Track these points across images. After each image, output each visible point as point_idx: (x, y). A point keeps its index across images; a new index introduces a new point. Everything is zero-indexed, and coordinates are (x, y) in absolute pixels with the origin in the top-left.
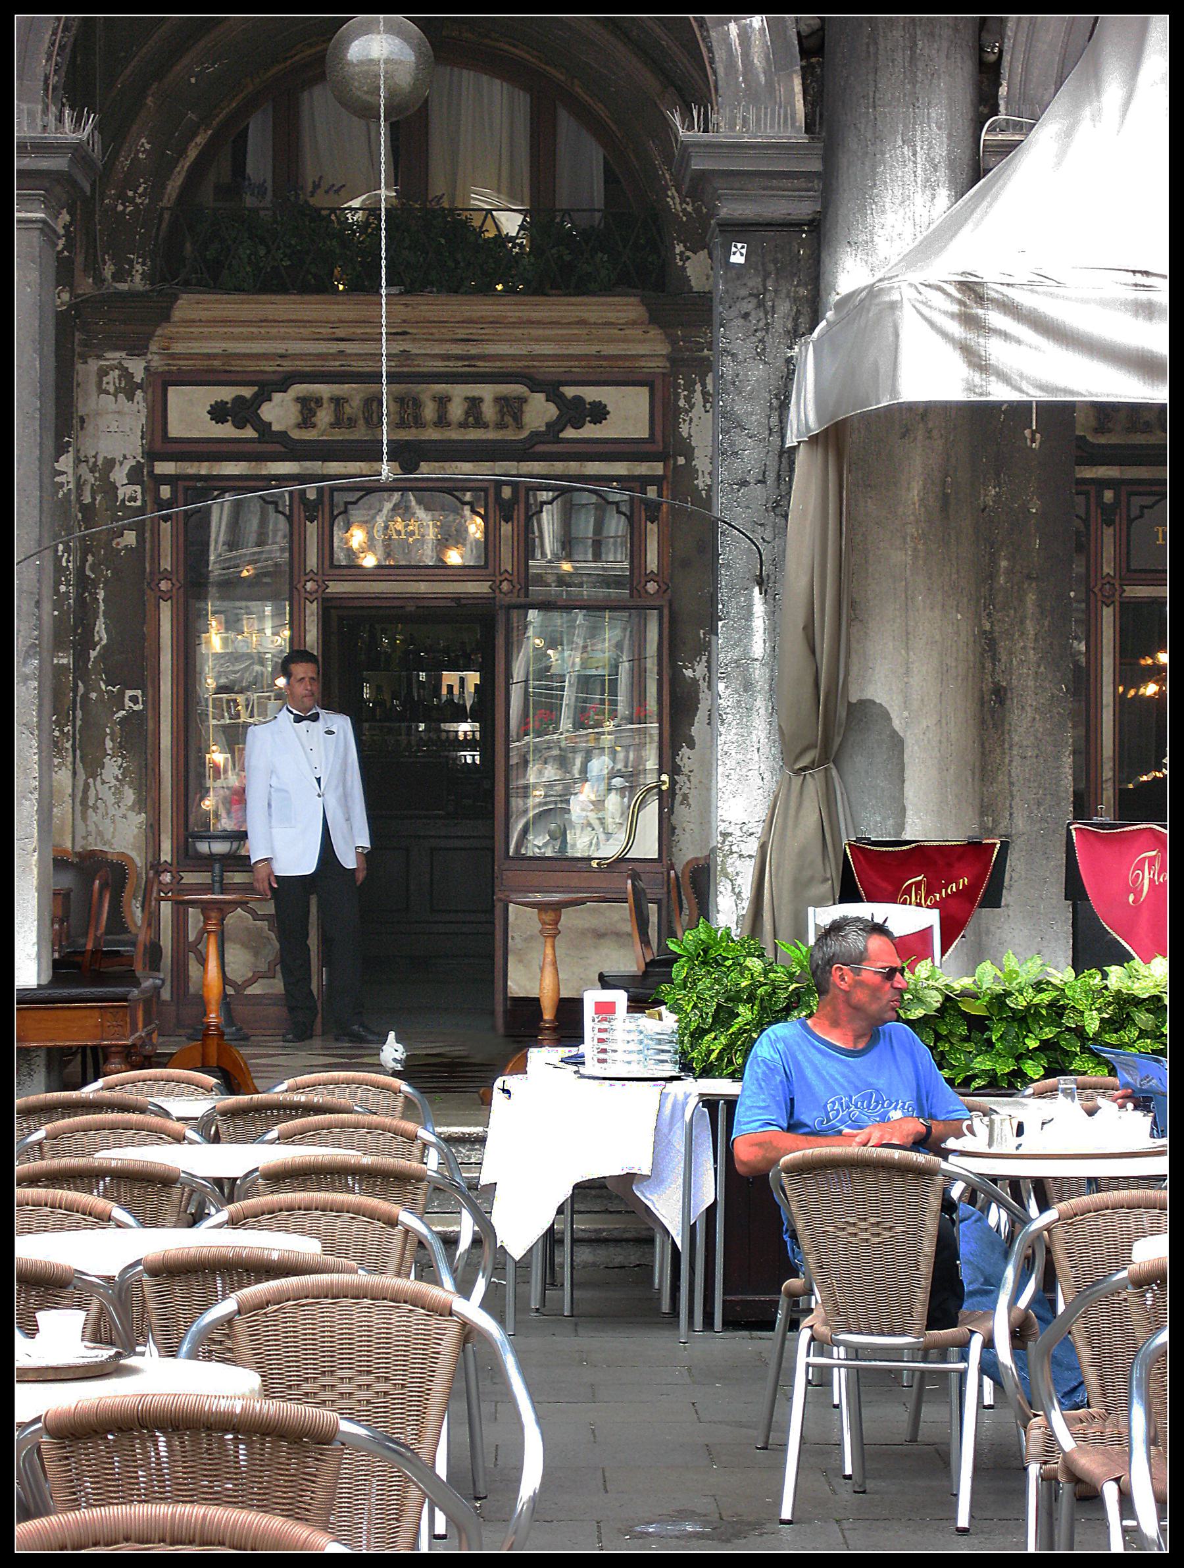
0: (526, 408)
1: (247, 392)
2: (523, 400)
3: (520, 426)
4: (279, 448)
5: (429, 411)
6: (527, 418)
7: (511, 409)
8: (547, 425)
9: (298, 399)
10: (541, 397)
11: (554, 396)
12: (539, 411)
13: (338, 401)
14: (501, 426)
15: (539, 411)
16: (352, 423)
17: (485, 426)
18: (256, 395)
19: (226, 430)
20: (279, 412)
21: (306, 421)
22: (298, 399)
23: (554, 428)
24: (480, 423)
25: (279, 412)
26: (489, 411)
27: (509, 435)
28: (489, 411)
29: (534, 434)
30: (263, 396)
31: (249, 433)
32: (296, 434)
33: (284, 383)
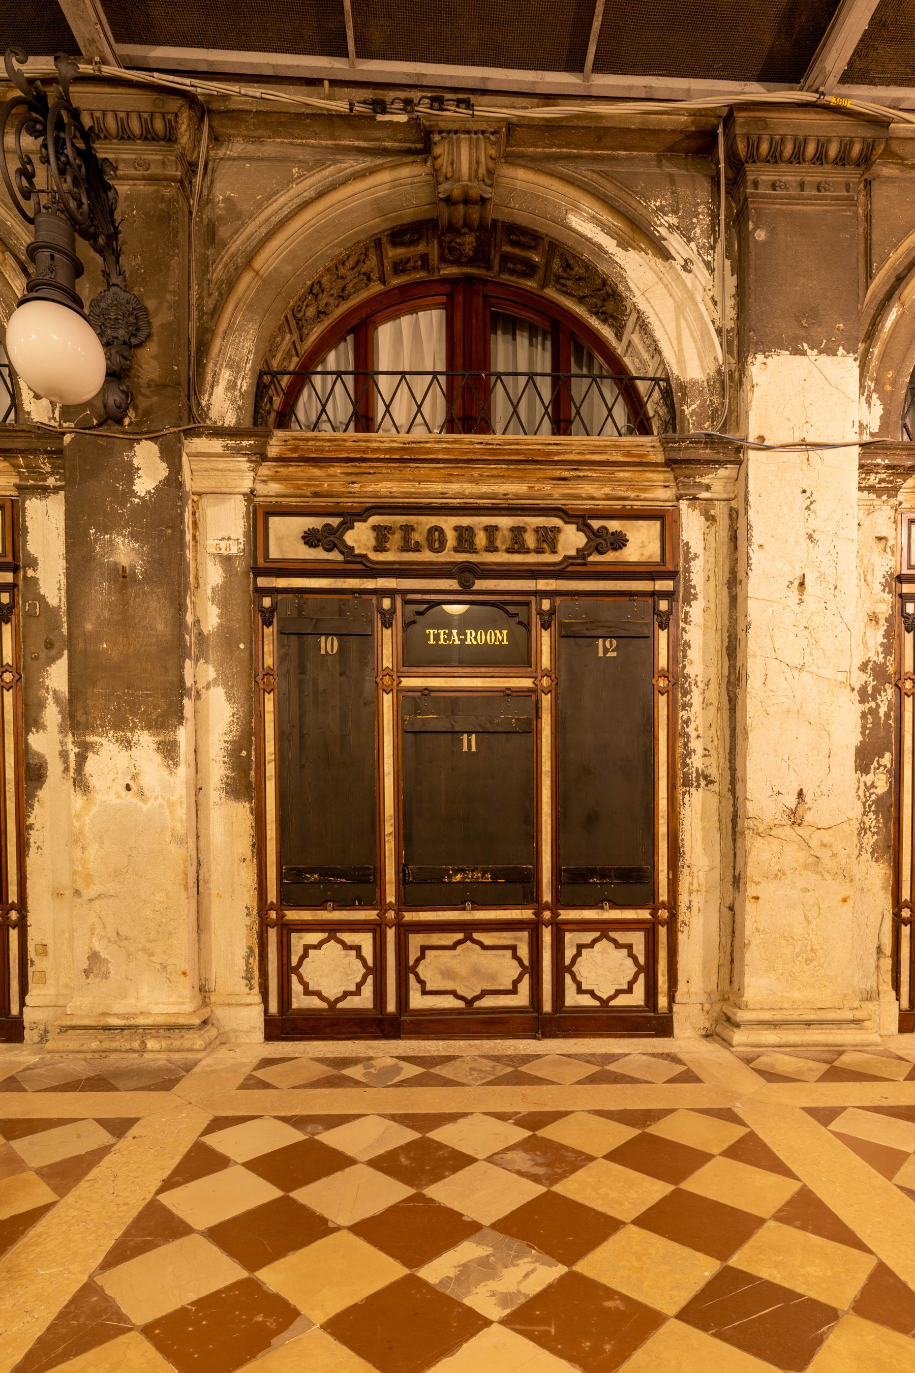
0: (562, 537)
1: (335, 521)
2: (558, 530)
3: (554, 552)
4: (361, 567)
5: (481, 539)
6: (560, 547)
7: (548, 538)
8: (578, 550)
9: (375, 528)
10: (574, 527)
11: (584, 527)
12: (572, 539)
13: (408, 529)
14: (539, 551)
15: (572, 539)
16: (417, 548)
17: (528, 551)
18: (342, 524)
19: (319, 554)
20: (360, 537)
21: (380, 547)
22: (375, 528)
23: (582, 553)
24: (524, 550)
25: (360, 537)
26: (530, 541)
27: (548, 558)
28: (530, 541)
29: (567, 558)
30: (347, 525)
31: (335, 556)
32: (373, 556)
33: (362, 514)
